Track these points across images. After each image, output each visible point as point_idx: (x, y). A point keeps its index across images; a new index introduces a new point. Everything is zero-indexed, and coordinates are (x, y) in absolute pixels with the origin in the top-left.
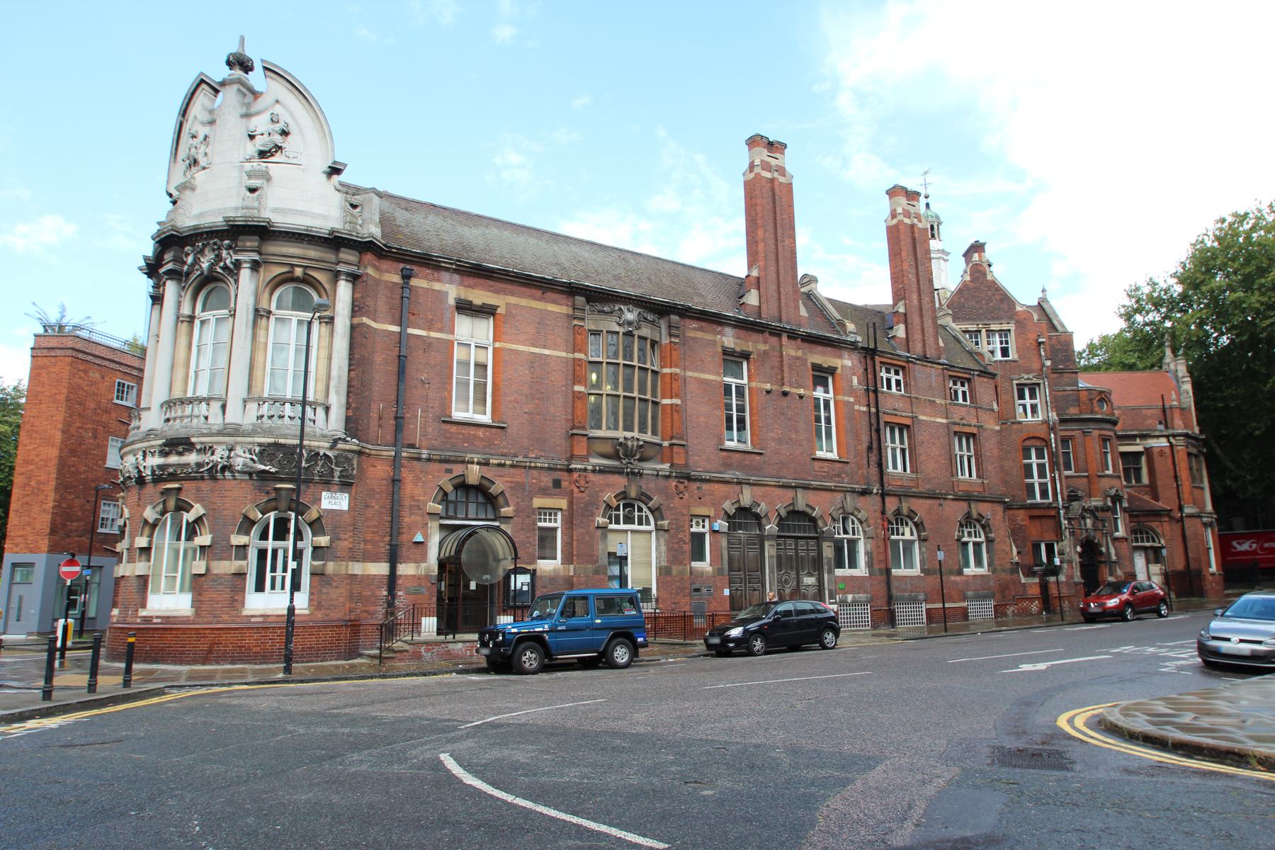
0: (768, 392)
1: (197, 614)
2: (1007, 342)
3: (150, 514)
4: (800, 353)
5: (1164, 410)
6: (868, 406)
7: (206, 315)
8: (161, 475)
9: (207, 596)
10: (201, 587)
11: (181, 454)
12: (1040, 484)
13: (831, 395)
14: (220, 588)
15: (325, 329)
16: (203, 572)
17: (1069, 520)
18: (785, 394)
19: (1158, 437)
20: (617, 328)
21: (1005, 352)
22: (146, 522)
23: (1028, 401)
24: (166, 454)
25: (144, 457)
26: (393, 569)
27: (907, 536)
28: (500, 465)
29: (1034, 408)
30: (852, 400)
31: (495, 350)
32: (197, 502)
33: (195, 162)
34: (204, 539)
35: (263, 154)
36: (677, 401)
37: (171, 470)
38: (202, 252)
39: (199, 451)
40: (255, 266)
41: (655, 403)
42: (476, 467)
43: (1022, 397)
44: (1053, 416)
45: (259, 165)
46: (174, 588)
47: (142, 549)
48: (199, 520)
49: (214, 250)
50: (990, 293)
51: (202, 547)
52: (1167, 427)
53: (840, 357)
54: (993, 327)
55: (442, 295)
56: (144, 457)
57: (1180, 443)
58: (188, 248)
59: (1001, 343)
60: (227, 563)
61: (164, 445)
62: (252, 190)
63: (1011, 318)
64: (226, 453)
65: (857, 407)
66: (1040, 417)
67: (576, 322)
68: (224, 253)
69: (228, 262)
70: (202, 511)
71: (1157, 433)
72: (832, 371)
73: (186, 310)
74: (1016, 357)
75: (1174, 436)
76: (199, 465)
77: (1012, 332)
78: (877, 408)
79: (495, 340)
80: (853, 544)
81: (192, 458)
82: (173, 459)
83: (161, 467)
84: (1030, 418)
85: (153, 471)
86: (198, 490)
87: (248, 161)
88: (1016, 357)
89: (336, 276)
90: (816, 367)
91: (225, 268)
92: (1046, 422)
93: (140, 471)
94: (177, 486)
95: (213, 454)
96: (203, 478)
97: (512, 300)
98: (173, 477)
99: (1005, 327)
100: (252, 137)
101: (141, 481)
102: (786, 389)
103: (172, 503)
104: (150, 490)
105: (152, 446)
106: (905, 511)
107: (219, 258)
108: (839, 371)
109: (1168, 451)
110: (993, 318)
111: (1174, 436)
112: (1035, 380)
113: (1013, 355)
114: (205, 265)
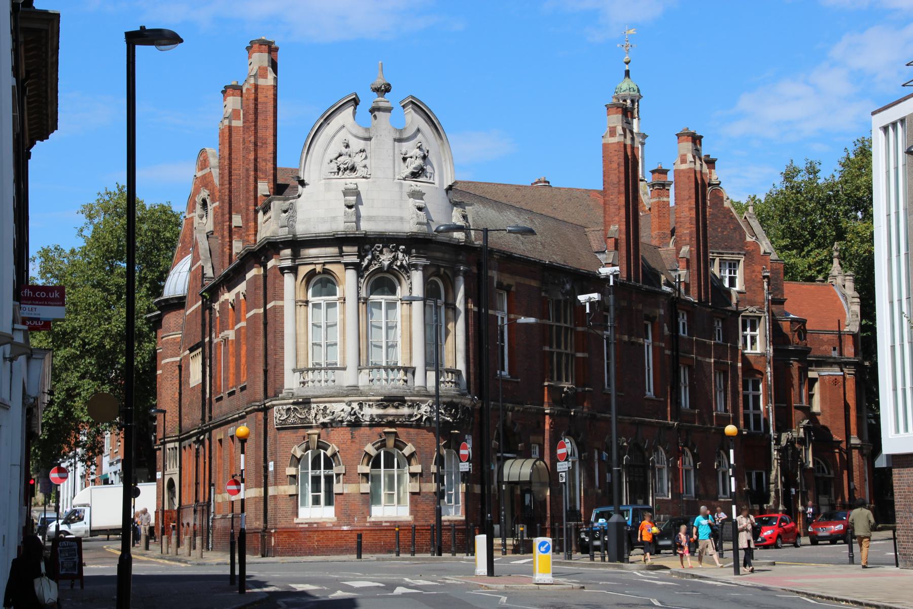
0: (625, 342)
1: (415, 519)
2: (735, 273)
3: (370, 449)
4: (640, 307)
5: (840, 338)
6: (672, 350)
7: (375, 298)
8: (373, 424)
9: (421, 507)
10: (416, 501)
11: (397, 408)
12: (754, 415)
13: (650, 340)
14: (428, 501)
15: (450, 313)
16: (418, 491)
17: (778, 450)
18: (633, 343)
19: (831, 364)
20: (561, 297)
21: (732, 282)
22: (367, 453)
23: (748, 332)
24: (385, 407)
25: (361, 408)
26: (483, 489)
27: (687, 466)
28: (518, 411)
29: (753, 339)
30: (663, 345)
31: (509, 320)
32: (409, 442)
33: (353, 169)
34: (417, 468)
35: (415, 175)
36: (586, 355)
37: (391, 419)
38: (381, 252)
39: (409, 406)
40: (425, 268)
41: (573, 355)
42: (510, 413)
43: (744, 329)
44: (770, 350)
45: (412, 185)
46: (392, 501)
47: (364, 474)
48: (412, 455)
49: (392, 252)
50: (725, 221)
51: (413, 475)
52: (841, 354)
53: (658, 307)
54: (726, 257)
55: (492, 278)
56: (361, 408)
57: (849, 371)
58: (367, 247)
59: (730, 273)
60: (429, 484)
61: (382, 400)
62: (420, 209)
63: (742, 249)
64: (429, 409)
65: (667, 352)
66: (759, 349)
67: (543, 294)
68: (400, 255)
69: (404, 262)
70: (414, 449)
71: (832, 360)
72: (652, 319)
73: (363, 294)
74: (743, 289)
75: (846, 364)
76: (411, 416)
77: (741, 263)
78: (677, 351)
79: (509, 312)
80: (660, 470)
81: (405, 411)
82: (391, 411)
83: (379, 416)
84: (748, 350)
85: (372, 419)
86: (408, 434)
87: (404, 179)
88: (743, 289)
89: (456, 273)
90: (648, 318)
91: (402, 266)
92: (763, 355)
93: (357, 417)
94: (393, 430)
95: (419, 409)
96: (411, 426)
97: (519, 279)
98: (391, 424)
99: (735, 257)
100: (405, 159)
101: (356, 424)
102: (633, 339)
103: (391, 442)
104: (364, 431)
105: (370, 401)
106: (690, 444)
107: (396, 258)
108: (657, 320)
109: (841, 380)
110: (726, 248)
111: (846, 364)
112: (758, 314)
113: (739, 286)
114: (386, 263)
